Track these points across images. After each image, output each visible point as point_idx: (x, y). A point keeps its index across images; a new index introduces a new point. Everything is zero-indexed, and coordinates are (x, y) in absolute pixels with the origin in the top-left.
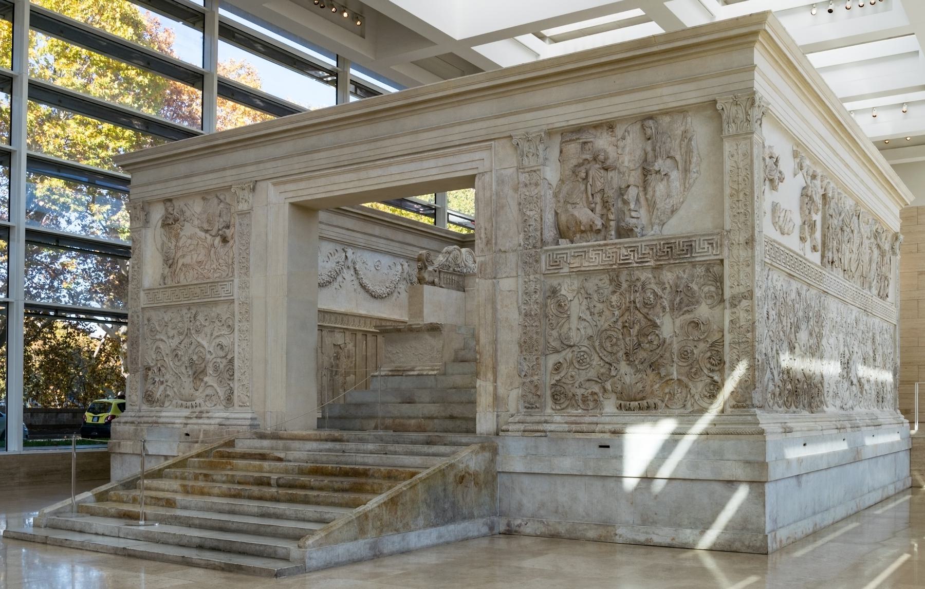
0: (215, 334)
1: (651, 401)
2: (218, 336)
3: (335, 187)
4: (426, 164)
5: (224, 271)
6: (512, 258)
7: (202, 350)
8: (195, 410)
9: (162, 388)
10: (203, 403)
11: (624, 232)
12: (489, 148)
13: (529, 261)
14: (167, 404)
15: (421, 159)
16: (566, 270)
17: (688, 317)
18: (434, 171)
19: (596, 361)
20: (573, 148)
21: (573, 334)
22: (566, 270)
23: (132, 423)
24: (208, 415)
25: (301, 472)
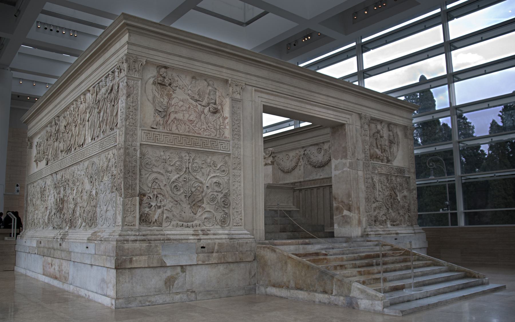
0: (212, 175)
1: (398, 222)
2: (214, 177)
3: (289, 106)
4: (330, 112)
5: (213, 132)
6: (361, 163)
7: (200, 185)
8: (195, 228)
9: (159, 211)
10: (202, 224)
11: (388, 161)
12: (351, 115)
13: (366, 166)
14: (165, 224)
15: (328, 109)
16: (376, 172)
17: (403, 194)
18: (332, 116)
19: (385, 208)
20: (373, 126)
21: (377, 196)
22: (376, 172)
23: (144, 240)
24: (212, 232)
25: (362, 258)
